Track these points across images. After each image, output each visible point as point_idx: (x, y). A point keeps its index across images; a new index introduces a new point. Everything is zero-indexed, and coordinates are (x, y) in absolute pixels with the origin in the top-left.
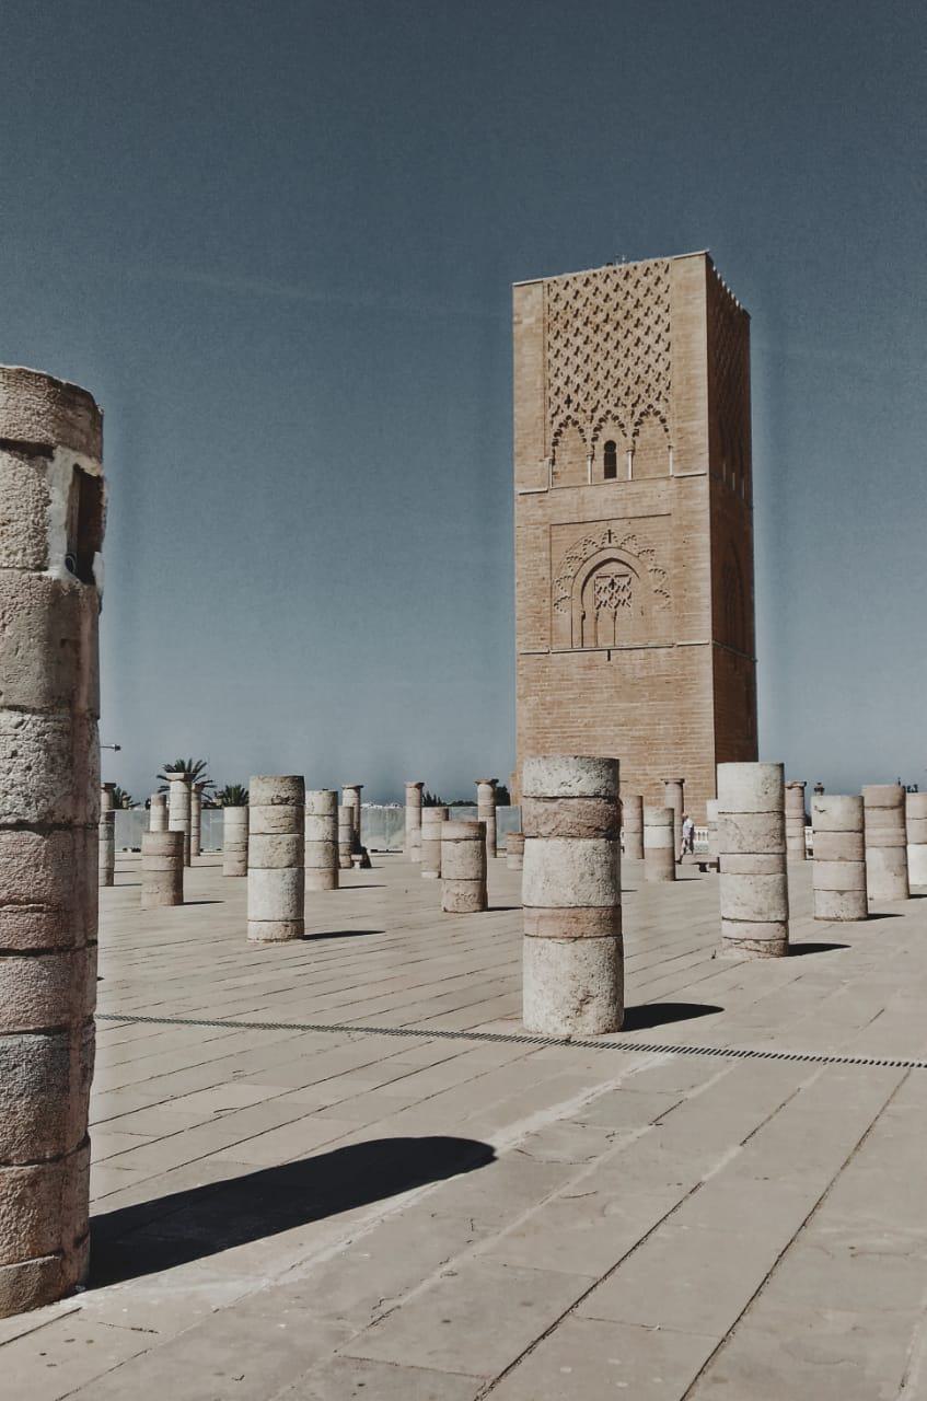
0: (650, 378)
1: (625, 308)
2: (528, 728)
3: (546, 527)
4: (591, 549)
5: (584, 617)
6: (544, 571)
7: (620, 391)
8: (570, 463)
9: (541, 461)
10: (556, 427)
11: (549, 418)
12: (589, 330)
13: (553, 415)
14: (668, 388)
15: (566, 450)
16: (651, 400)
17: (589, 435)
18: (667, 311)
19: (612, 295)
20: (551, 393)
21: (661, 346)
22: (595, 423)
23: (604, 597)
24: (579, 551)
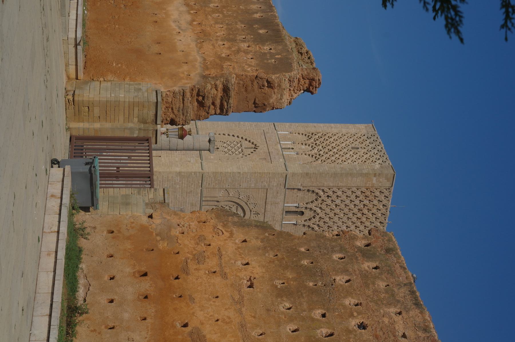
2: (163, 176)
3: (267, 187)
4: (251, 207)
5: (218, 201)
8: (297, 196)
9: (301, 185)
10: (317, 191)
11: (323, 188)
15: (304, 194)
17: (309, 206)
20: (335, 189)
22: (314, 208)
24: (252, 201)
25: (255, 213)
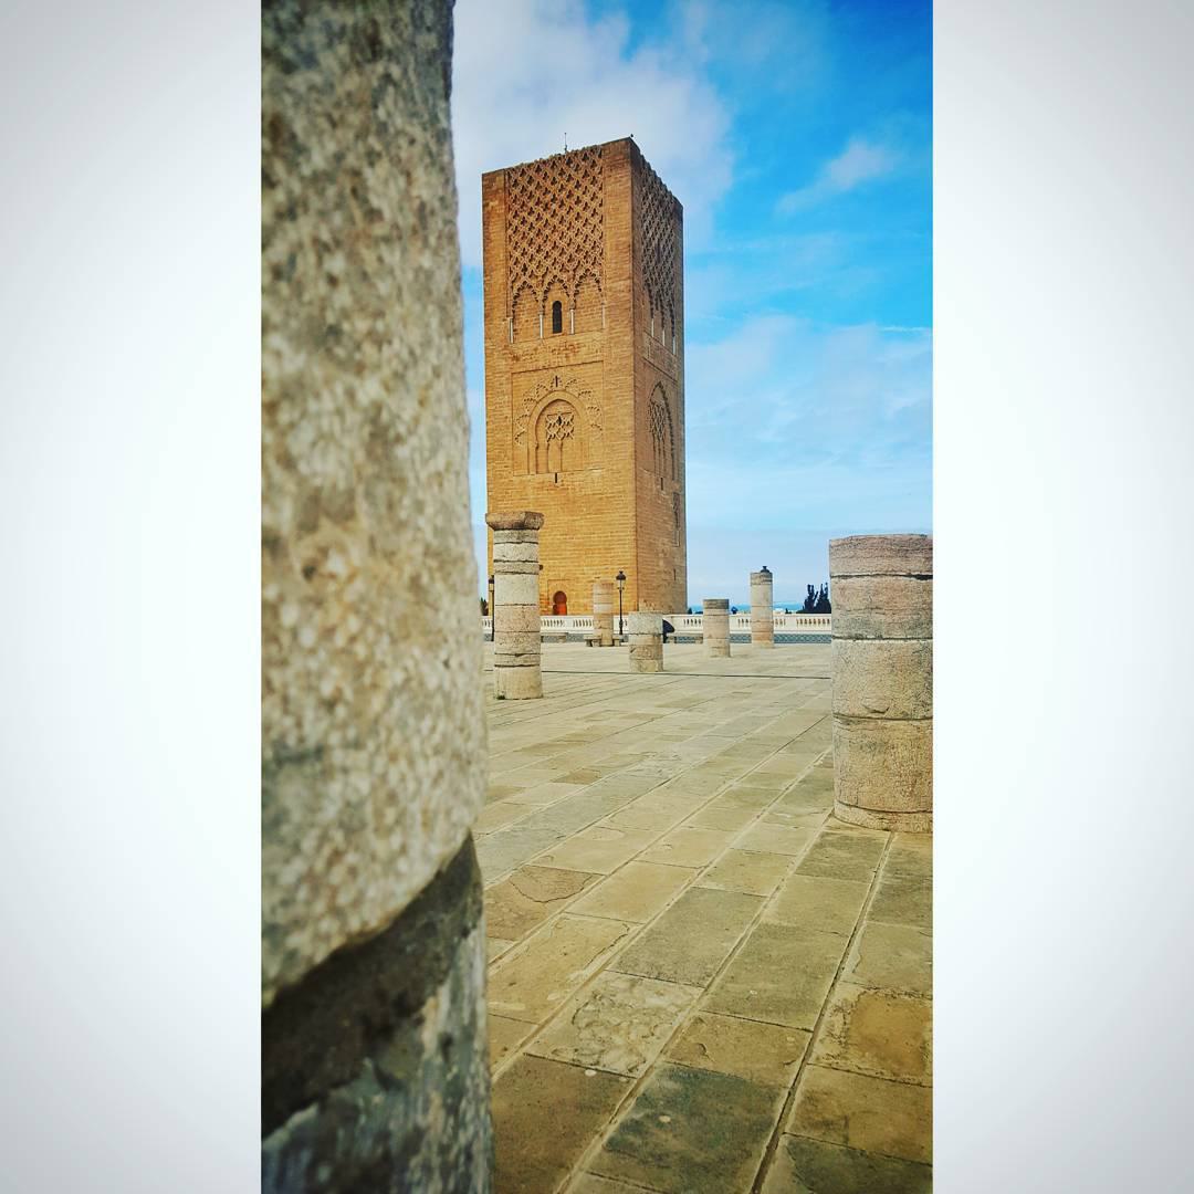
0: (588, 247)
1: (568, 188)
5: (537, 448)
6: (507, 411)
7: (564, 259)
10: (515, 291)
11: (510, 284)
12: (539, 209)
13: (513, 282)
14: (601, 254)
16: (588, 266)
17: (540, 298)
18: (601, 189)
19: (558, 178)
20: (511, 263)
21: (596, 220)
23: (553, 432)
25: (554, 385)
